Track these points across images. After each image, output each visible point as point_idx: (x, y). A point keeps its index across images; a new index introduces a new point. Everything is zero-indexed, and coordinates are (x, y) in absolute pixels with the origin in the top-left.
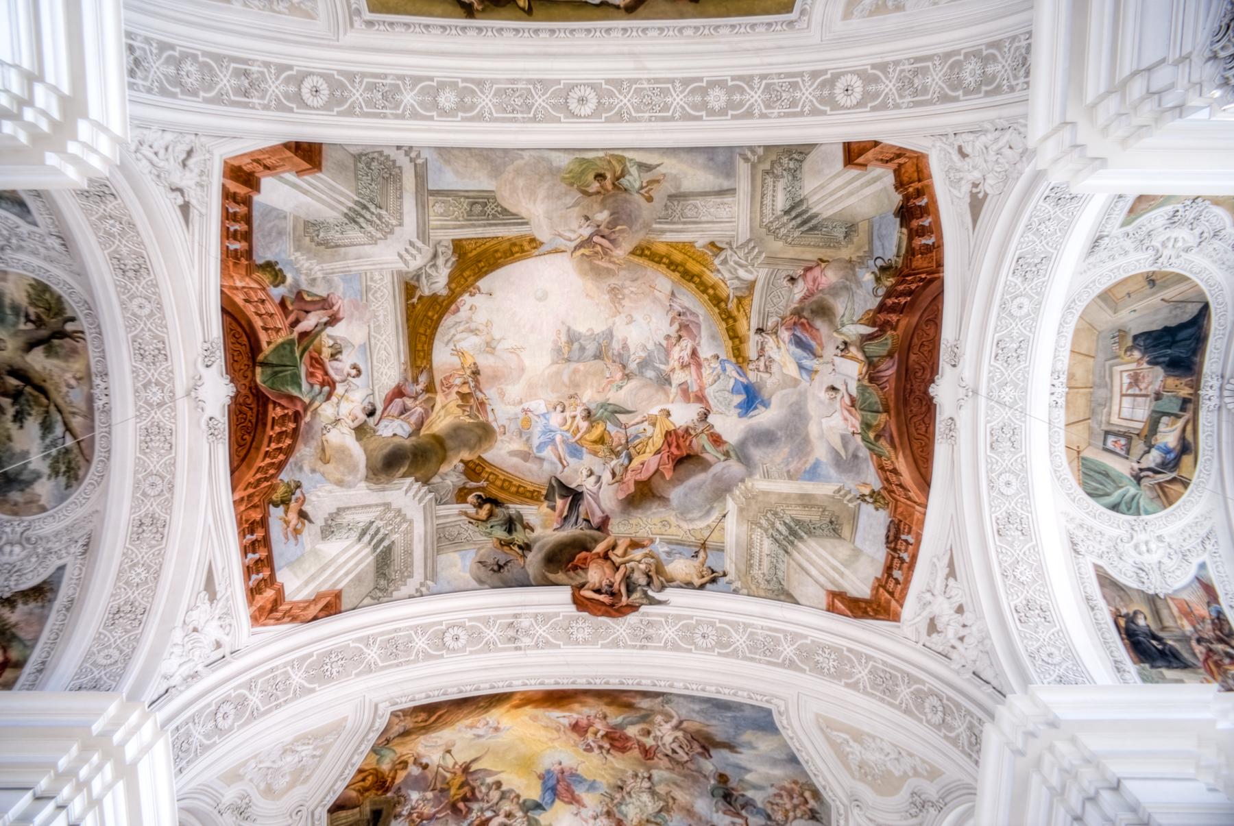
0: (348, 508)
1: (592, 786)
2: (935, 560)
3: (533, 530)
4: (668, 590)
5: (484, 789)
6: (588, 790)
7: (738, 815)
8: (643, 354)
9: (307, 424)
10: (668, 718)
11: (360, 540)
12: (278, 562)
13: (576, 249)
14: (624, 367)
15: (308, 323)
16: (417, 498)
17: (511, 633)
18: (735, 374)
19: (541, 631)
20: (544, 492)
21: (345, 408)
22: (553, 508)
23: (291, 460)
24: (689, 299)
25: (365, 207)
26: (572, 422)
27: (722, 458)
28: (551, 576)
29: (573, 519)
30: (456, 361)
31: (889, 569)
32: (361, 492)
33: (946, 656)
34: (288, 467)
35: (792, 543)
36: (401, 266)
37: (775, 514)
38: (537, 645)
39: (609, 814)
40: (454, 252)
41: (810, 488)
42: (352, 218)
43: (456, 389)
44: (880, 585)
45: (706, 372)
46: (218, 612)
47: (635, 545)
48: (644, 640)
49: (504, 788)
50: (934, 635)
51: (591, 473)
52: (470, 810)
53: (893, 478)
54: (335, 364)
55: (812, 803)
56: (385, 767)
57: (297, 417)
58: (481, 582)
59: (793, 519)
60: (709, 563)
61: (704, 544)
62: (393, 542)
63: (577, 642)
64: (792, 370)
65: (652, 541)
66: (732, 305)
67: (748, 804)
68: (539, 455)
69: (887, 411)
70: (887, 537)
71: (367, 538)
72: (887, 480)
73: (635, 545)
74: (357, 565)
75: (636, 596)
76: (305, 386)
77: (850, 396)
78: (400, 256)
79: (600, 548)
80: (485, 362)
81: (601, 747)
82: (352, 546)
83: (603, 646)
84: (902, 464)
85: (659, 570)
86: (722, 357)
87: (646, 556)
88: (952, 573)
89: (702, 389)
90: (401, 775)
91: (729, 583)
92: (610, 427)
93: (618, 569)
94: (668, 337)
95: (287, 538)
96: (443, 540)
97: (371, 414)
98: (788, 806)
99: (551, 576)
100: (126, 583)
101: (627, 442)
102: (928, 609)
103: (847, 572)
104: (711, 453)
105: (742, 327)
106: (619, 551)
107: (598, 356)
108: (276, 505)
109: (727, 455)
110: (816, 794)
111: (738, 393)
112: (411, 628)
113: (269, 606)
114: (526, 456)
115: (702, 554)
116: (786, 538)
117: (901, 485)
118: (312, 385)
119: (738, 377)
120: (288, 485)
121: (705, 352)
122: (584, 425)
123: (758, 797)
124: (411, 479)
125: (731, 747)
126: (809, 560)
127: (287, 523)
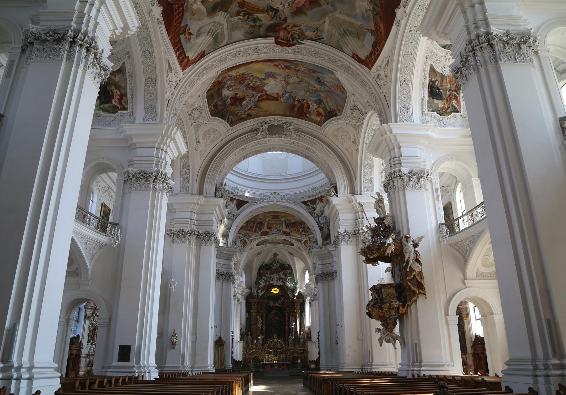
0: (203, 27)
1: (280, 75)
2: (384, 59)
3: (262, 21)
4: (305, 40)
5: (248, 77)
6: (279, 76)
7: (322, 86)
9: (187, 6)
10: (303, 66)
11: (208, 35)
12: (185, 51)
17: (256, 51)
19: (265, 50)
20: (266, 10)
22: (269, 15)
27: (326, 4)
28: (268, 34)
29: (275, 18)
31: (371, 54)
32: (207, 20)
34: (183, 21)
35: (345, 36)
37: (341, 25)
38: (264, 53)
39: (285, 81)
41: (353, 21)
44: (367, 58)
46: (174, 74)
47: (295, 26)
48: (297, 52)
49: (254, 76)
50: (378, 79)
51: (281, 4)
52: (245, 82)
53: (378, 29)
55: (342, 90)
56: (220, 79)
58: (245, 37)
59: (346, 29)
61: (317, 29)
62: (218, 32)
63: (276, 52)
65: (301, 25)
69: (381, 8)
70: (373, 45)
71: (210, 33)
72: (377, 28)
73: (295, 26)
74: (208, 42)
75: (295, 41)
79: (284, 26)
81: (283, 69)
82: (206, 37)
83: (284, 53)
84: (382, 25)
85: (303, 33)
87: (298, 29)
88: (387, 64)
90: (224, 80)
91: (324, 41)
93: (289, 33)
95: (187, 43)
96: (233, 28)
98: (336, 88)
100: (147, 71)
102: (378, 72)
103: (359, 50)
106: (290, 27)
108: (182, 34)
109: (328, 3)
110: (344, 89)
112: (226, 55)
113: (186, 64)
115: (316, 31)
116: (343, 34)
117: (380, 32)
123: (328, 84)
124: (222, 11)
126: (349, 42)
127: (186, 38)
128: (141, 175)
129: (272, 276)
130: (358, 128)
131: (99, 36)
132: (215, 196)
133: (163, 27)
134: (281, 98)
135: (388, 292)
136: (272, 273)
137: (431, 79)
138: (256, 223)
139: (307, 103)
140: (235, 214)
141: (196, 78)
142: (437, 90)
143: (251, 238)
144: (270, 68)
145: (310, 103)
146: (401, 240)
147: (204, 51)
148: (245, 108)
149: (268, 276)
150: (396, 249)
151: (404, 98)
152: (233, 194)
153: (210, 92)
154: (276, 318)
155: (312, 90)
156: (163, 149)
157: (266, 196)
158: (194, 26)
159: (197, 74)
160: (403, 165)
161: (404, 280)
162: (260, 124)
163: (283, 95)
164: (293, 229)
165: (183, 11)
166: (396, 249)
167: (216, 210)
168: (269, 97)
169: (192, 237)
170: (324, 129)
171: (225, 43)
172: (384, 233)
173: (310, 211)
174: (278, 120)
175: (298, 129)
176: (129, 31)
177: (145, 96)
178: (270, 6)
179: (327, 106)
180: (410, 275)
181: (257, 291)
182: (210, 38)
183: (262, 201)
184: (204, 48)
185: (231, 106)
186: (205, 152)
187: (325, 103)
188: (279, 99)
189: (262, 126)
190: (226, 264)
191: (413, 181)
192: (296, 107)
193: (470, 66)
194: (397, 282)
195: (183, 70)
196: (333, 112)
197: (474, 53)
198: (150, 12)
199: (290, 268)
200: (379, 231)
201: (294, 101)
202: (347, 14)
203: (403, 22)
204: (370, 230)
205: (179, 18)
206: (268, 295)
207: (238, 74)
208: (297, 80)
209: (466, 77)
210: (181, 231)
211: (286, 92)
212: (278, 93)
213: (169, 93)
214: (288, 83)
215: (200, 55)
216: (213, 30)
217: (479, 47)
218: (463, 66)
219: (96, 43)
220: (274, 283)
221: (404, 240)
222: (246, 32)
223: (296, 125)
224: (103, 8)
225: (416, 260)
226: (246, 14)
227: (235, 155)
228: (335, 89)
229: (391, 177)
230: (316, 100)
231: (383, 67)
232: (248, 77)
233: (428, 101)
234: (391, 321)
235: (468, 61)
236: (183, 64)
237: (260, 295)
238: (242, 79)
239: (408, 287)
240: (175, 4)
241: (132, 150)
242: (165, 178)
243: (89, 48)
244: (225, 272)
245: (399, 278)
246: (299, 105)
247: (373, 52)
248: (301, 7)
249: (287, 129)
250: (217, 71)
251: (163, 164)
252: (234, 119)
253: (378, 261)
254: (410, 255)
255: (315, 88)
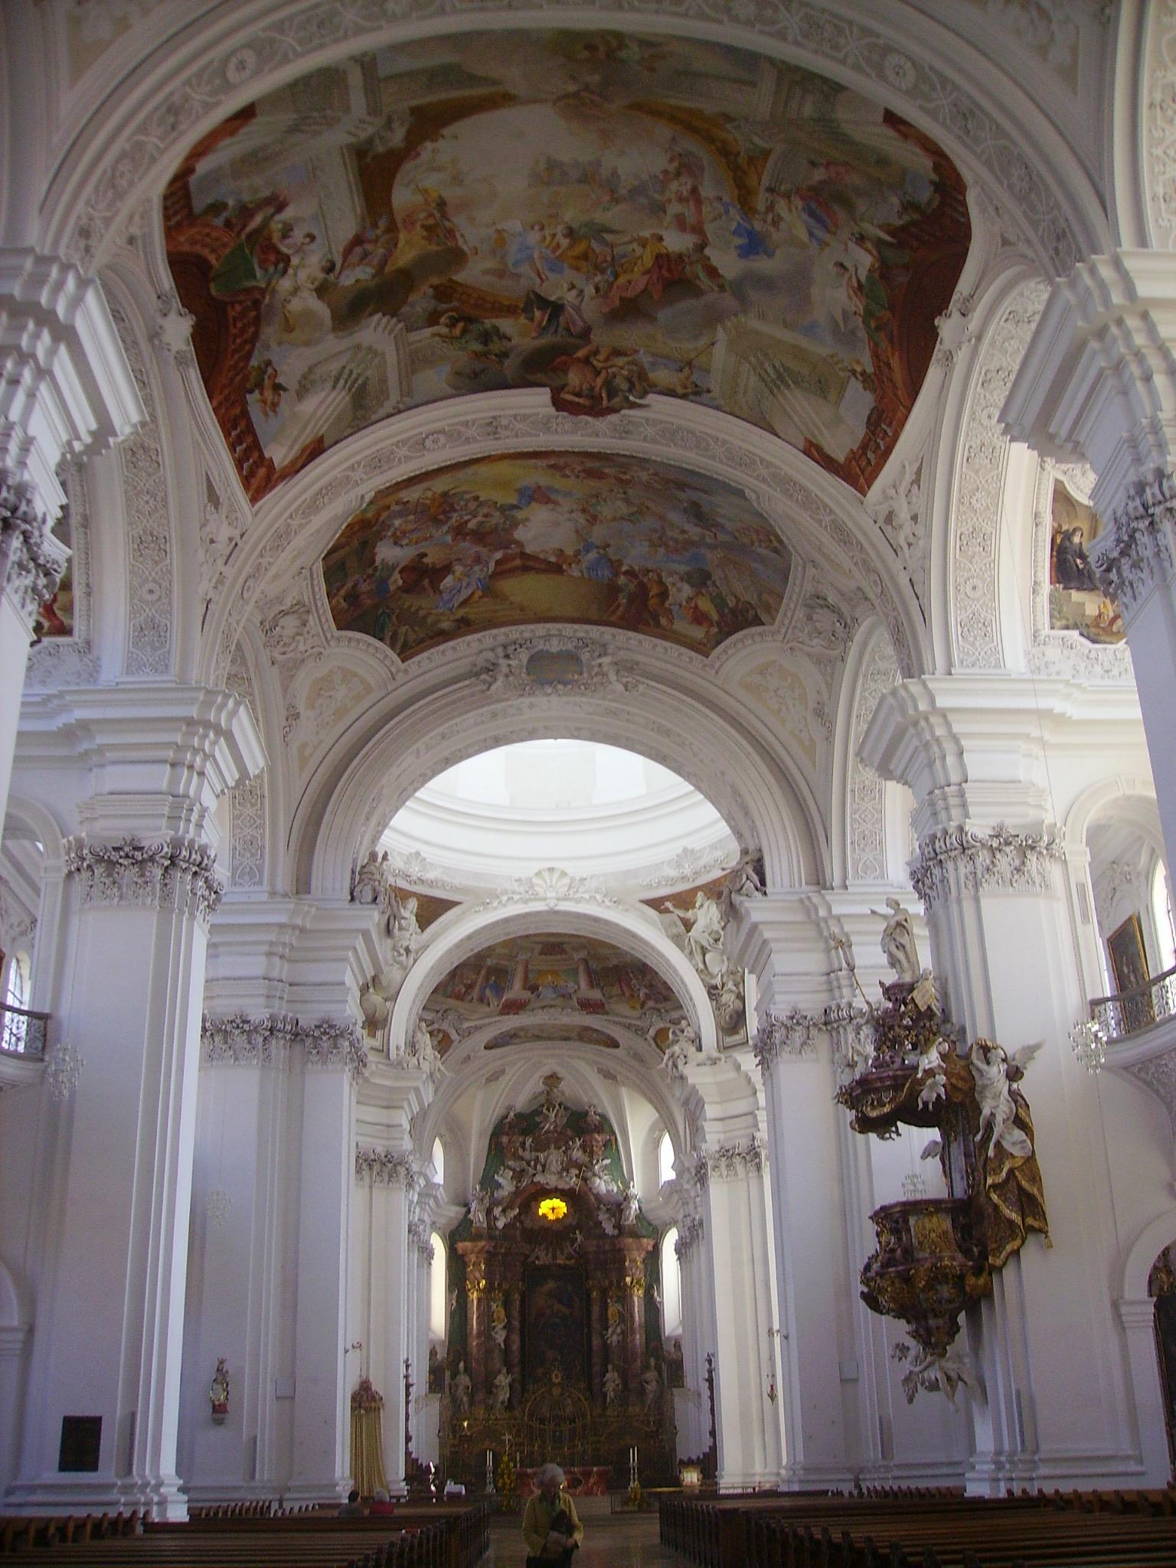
8: (636, 183)
9: (270, 305)
10: (644, 469)
11: (334, 387)
13: (559, 99)
14: (612, 191)
15: (258, 220)
16: (386, 332)
17: (489, 429)
18: (738, 217)
21: (302, 275)
22: (532, 319)
23: (258, 345)
24: (690, 145)
25: (307, 118)
26: (551, 242)
27: (716, 289)
28: (530, 377)
29: (552, 330)
30: (419, 198)
31: (864, 447)
32: (332, 343)
33: (895, 551)
35: (778, 387)
36: (353, 140)
37: (766, 355)
39: (584, 511)
40: (411, 115)
41: (803, 342)
42: (294, 129)
43: (419, 223)
45: (705, 209)
46: (224, 516)
47: (617, 353)
49: (481, 499)
51: (573, 287)
54: (287, 241)
55: (775, 543)
56: (369, 515)
57: (257, 304)
58: (456, 388)
60: (695, 377)
64: (802, 234)
65: (636, 352)
66: (742, 160)
67: (717, 525)
68: (514, 271)
70: (869, 418)
71: (342, 382)
72: (879, 367)
73: (617, 353)
75: (616, 400)
76: (259, 273)
77: (859, 281)
78: (350, 133)
79: (580, 354)
80: (448, 194)
81: (578, 477)
82: (328, 395)
84: (895, 362)
85: (642, 375)
86: (726, 199)
87: (628, 363)
88: (917, 481)
89: (700, 223)
92: (594, 244)
93: (598, 373)
94: (665, 172)
95: (266, 415)
96: (415, 362)
97: (330, 268)
99: (530, 377)
101: (613, 259)
103: (825, 431)
104: (704, 281)
105: (752, 181)
106: (601, 357)
107: (584, 179)
108: (251, 392)
109: (722, 288)
110: (781, 542)
111: (740, 235)
114: (501, 274)
115: (686, 370)
116: (773, 381)
118: (266, 270)
119: (741, 221)
120: (259, 368)
121: (707, 191)
122: (565, 242)
123: (729, 525)
125: (706, 492)
127: (264, 402)
128: (122, 853)
129: (542, 1156)
130: (829, 665)
131: (37, 481)
132: (353, 899)
133: (194, 375)
134: (570, 564)
135: (928, 1226)
136: (541, 1146)
137: (1060, 526)
138: (483, 972)
139: (660, 583)
140: (413, 947)
141: (294, 523)
142: (1078, 561)
143: (466, 1025)
144: (536, 476)
145: (668, 581)
146: (967, 1057)
147: (322, 437)
148: (451, 600)
149: (527, 1155)
150: (954, 1086)
151: (974, 588)
152: (406, 876)
153: (336, 556)
154: (557, 1306)
155: (676, 541)
156: (191, 767)
157: (519, 880)
158: (290, 365)
159: (296, 511)
160: (972, 810)
161: (979, 1185)
162: (500, 651)
163: (577, 553)
164: (616, 990)
165: (257, 322)
166: (950, 1088)
167: (355, 948)
168: (530, 564)
169: (274, 1042)
170: (717, 665)
171: (388, 407)
172: (913, 1033)
173: (675, 931)
174: (557, 637)
175: (629, 665)
176: (111, 440)
177: (133, 590)
178: (537, 295)
179: (724, 590)
180: (997, 1170)
181: (489, 1212)
182: (340, 397)
183: (504, 898)
184: (322, 426)
185: (404, 595)
186: (316, 747)
187: (718, 583)
188: (564, 567)
189: (507, 656)
190: (385, 1121)
191: (1005, 862)
192: (621, 596)
193: (1142, 560)
194: (959, 1193)
195: (254, 500)
196: (748, 611)
197: (1152, 523)
198: (154, 335)
199: (603, 1125)
200: (897, 1029)
201: (617, 574)
202: (784, 321)
203: (961, 358)
204: (867, 1022)
205: (245, 342)
206: (528, 1224)
207: (429, 494)
208: (624, 509)
209: (1132, 587)
210: (238, 1021)
211: (588, 548)
212: (562, 551)
213: (210, 581)
214: (594, 519)
215: (309, 451)
216: (351, 372)
217: (1162, 507)
218: (1123, 553)
219: (29, 502)
220: (550, 1180)
221: (976, 1059)
222: (458, 374)
223: (621, 653)
224: (44, 389)
225: (1014, 1122)
226: (458, 321)
227: (418, 757)
228: (752, 543)
229: (935, 851)
230: (687, 573)
231: (902, 491)
232: (462, 503)
233: (1051, 595)
234: (941, 1322)
235: (1136, 545)
236: (255, 482)
237: (500, 1224)
238: (439, 511)
239: (990, 1211)
240: (233, 304)
241: (91, 770)
242: (201, 863)
243: (11, 520)
244: (381, 1150)
245: (962, 1178)
246: (632, 587)
247: (870, 439)
248: (637, 296)
249: (593, 667)
250: (360, 494)
251: (194, 817)
252: (412, 637)
253: (899, 1124)
254: (996, 1105)
255: (686, 536)
